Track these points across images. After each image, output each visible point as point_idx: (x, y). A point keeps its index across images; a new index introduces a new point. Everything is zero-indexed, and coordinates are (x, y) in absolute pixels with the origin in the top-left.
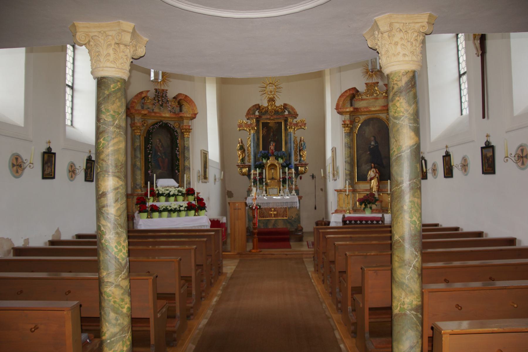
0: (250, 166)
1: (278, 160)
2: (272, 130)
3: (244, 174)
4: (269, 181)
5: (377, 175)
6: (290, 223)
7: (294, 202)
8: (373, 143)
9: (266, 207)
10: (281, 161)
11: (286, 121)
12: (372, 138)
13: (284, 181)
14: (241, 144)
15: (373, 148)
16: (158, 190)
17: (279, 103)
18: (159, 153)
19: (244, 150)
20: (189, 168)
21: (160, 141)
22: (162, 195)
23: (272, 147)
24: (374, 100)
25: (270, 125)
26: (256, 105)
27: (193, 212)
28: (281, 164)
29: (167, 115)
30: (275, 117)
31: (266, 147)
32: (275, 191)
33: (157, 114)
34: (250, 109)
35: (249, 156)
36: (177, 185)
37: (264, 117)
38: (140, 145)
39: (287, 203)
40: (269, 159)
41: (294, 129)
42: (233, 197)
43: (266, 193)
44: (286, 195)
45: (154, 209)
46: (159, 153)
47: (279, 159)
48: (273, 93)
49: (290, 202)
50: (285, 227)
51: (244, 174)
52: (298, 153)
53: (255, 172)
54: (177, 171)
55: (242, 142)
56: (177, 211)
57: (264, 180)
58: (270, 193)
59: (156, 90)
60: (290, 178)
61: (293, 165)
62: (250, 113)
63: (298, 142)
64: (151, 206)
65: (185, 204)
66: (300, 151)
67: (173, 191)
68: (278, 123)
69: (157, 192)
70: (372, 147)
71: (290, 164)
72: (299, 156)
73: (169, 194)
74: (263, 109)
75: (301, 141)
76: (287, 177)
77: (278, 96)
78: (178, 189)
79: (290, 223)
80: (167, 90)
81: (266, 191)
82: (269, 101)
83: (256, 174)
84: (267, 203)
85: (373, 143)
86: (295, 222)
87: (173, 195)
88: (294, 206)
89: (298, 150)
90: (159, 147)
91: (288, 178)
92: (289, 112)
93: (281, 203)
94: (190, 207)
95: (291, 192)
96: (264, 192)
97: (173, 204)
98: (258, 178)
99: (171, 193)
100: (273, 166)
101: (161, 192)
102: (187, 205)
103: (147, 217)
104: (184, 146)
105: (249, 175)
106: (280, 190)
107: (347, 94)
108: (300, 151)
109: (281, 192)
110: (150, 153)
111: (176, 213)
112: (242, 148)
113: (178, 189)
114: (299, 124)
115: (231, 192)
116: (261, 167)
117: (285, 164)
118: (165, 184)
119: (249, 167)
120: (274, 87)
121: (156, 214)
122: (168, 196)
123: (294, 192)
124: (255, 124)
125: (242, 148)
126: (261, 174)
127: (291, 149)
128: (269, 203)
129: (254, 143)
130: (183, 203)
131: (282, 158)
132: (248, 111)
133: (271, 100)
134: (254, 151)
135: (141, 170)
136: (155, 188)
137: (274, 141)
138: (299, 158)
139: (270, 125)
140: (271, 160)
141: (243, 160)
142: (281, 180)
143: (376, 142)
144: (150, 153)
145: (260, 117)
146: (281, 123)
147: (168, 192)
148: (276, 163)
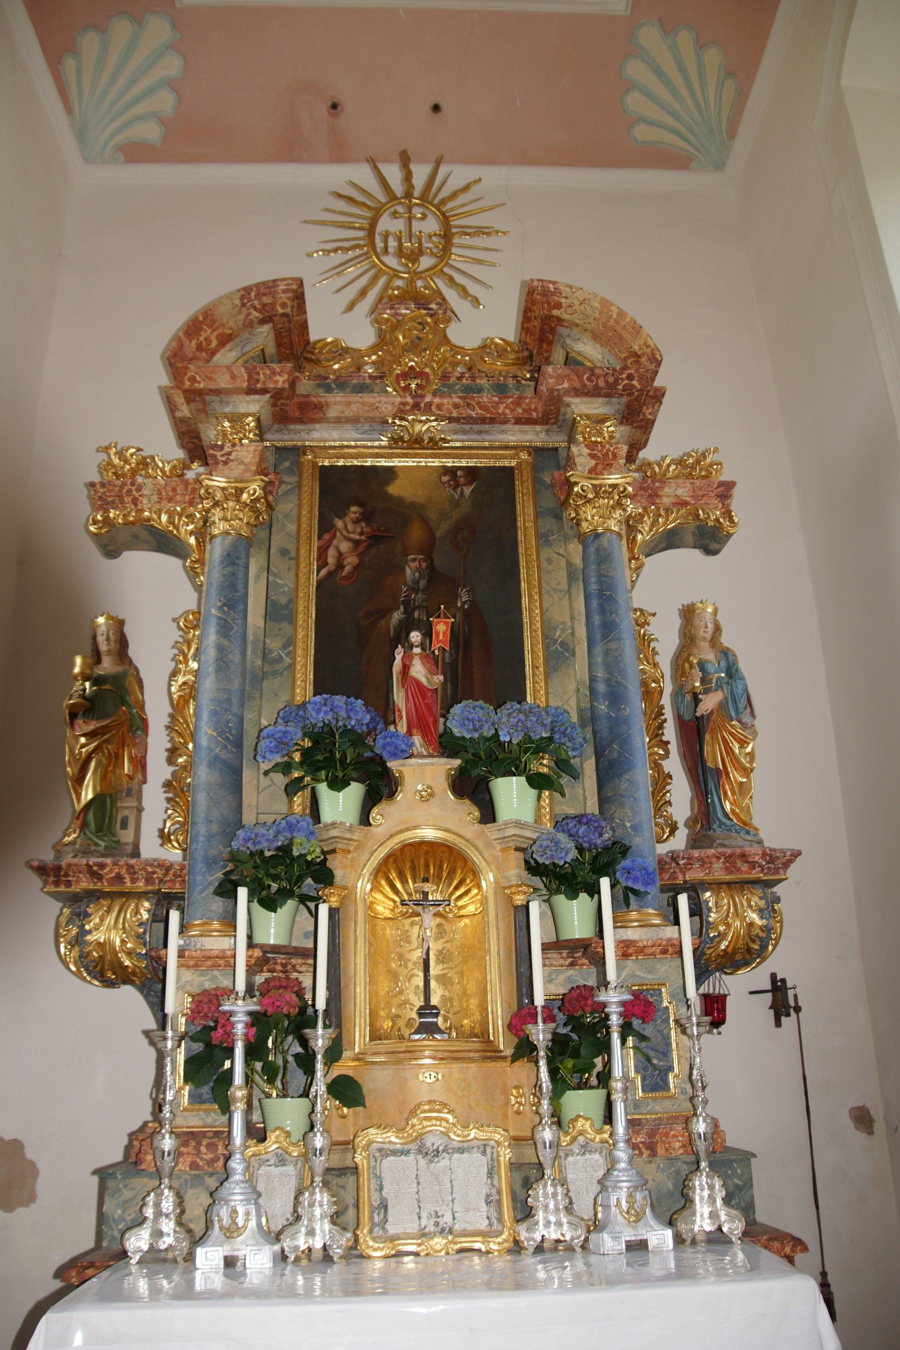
1: (488, 814)
2: (416, 533)
3: (104, 970)
25: (394, 489)
26: (269, 287)
31: (351, 653)
32: (466, 1186)
40: (380, 786)
53: (216, 943)
55: (122, 643)
57: (320, 1038)
63: (665, 661)
68: (472, 473)
76: (613, 999)
83: (227, 961)
91: (629, 1010)
100: (426, 865)
105: (152, 983)
108: (694, 732)
131: (538, 782)
139: (394, 489)
142: (540, 1033)
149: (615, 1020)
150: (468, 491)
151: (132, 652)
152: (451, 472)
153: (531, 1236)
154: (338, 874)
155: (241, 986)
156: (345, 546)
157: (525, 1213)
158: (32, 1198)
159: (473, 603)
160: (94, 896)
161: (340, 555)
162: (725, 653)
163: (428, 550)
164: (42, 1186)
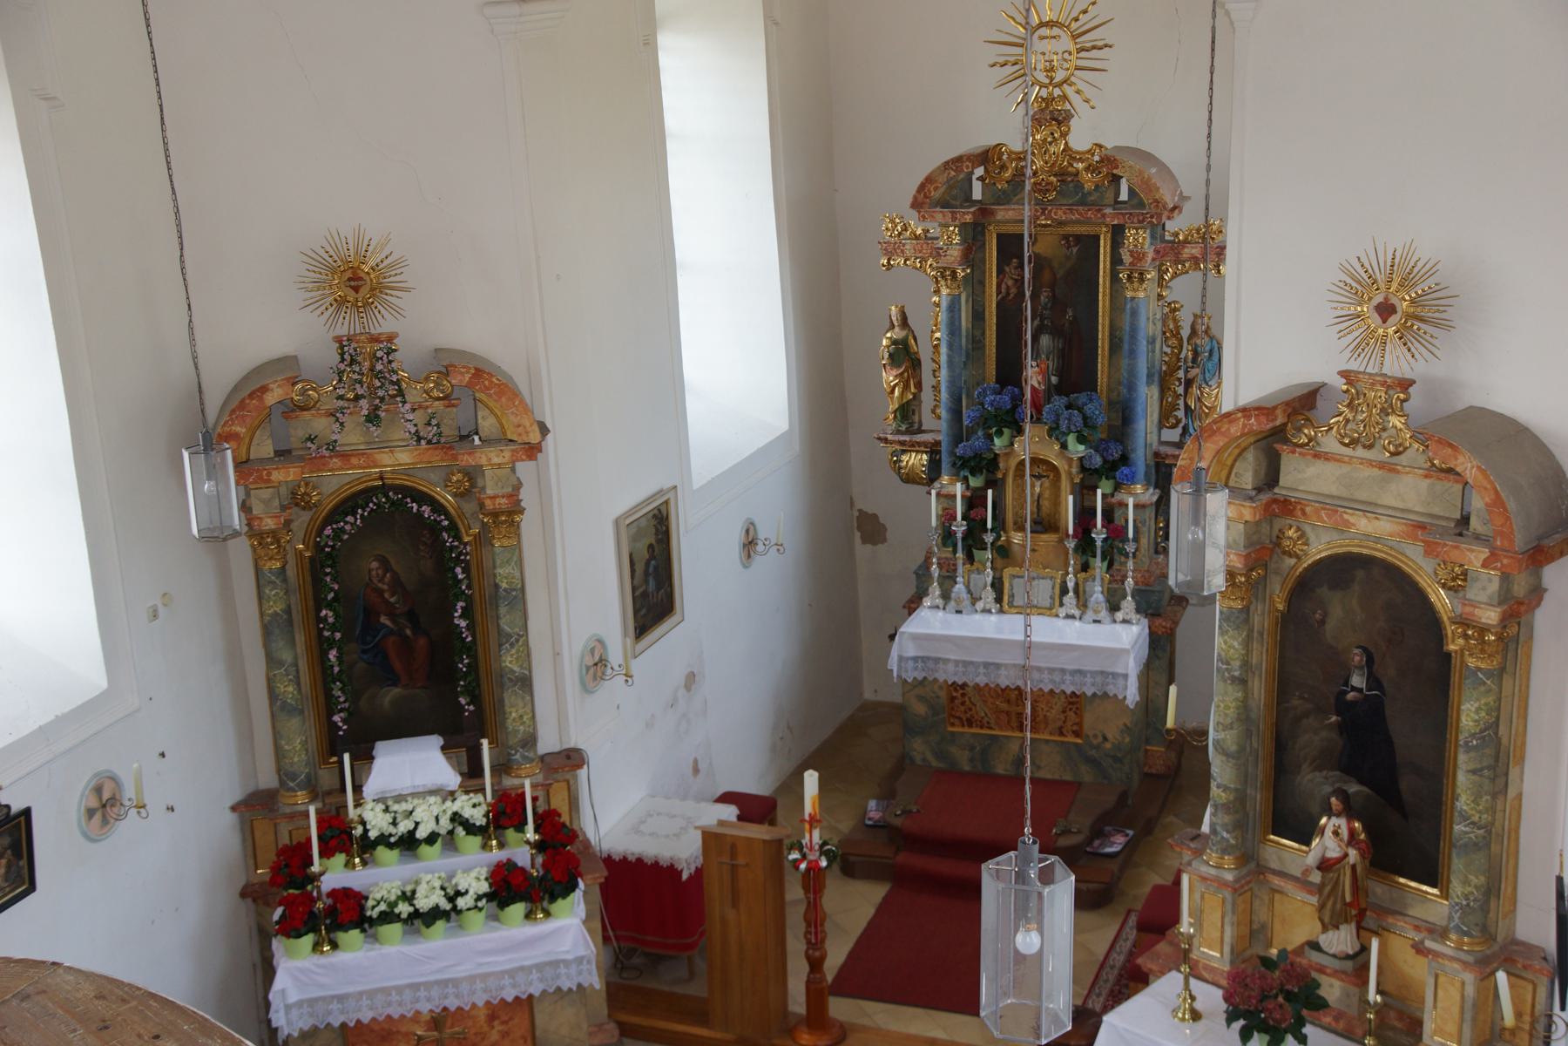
0: (938, 443)
3: (909, 478)
4: (1017, 538)
5: (1353, 854)
6: (1093, 762)
7: (1114, 675)
8: (1357, 680)
9: (981, 680)
10: (1077, 449)
11: (1118, 233)
12: (1357, 657)
13: (1085, 543)
14: (897, 333)
15: (1354, 703)
16: (363, 823)
17: (1080, 137)
18: (384, 620)
19: (916, 364)
20: (526, 683)
21: (384, 563)
22: (383, 840)
23: (1033, 376)
24: (1376, 472)
27: (518, 909)
28: (1081, 459)
29: (404, 457)
30: (1061, 215)
32: (1043, 590)
33: (354, 461)
34: (929, 180)
35: (936, 388)
36: (452, 779)
37: (1003, 213)
38: (288, 611)
39: (1080, 672)
41: (1161, 273)
42: (884, 540)
43: (999, 600)
44: (1090, 615)
45: (349, 913)
46: (384, 620)
47: (1071, 439)
48: (1059, 76)
49: (1094, 674)
50: (1068, 777)
51: (909, 478)
52: (1181, 390)
54: (463, 701)
55: (904, 322)
56: (446, 914)
58: (1018, 601)
59: (339, 340)
60: (1116, 533)
61: (1141, 458)
62: (944, 191)
63: (1185, 333)
64: (333, 893)
65: (475, 882)
66: (1189, 383)
67: (427, 817)
69: (359, 831)
70: (1351, 696)
71: (1125, 459)
72: (1181, 402)
73: (412, 833)
74: (1003, 167)
75: (1194, 332)
77: (1088, 92)
78: (452, 807)
79: (1093, 762)
80: (391, 338)
81: (997, 586)
82: (1037, 122)
84: (986, 665)
85: (1357, 680)
86: (1116, 759)
87: (432, 839)
88: (1111, 690)
89: (1181, 374)
90: (380, 592)
92: (1131, 192)
93: (1051, 670)
94: (507, 888)
95: (1114, 608)
96: (989, 595)
97: (427, 878)
98: (959, 527)
99: (421, 833)
101: (373, 834)
102: (484, 887)
103: (316, 947)
104: (497, 586)
106: (1064, 591)
107: (1235, 430)
109: (1070, 598)
110: (331, 643)
111: (440, 925)
112: (904, 355)
113: (452, 807)
114: (1188, 252)
115: (875, 516)
116: (983, 465)
117: (1098, 461)
118: (411, 774)
119: (933, 450)
120: (1066, 43)
121: (351, 937)
122: (408, 843)
123: (1128, 604)
124: (955, 253)
125: (904, 355)
126: (974, 502)
127: (1132, 387)
128: (998, 666)
129: (950, 346)
130: (471, 870)
131: (1081, 439)
132: (922, 187)
133: (1052, 116)
134: (952, 382)
135: (302, 712)
136: (352, 813)
137: (1056, 332)
138: (1181, 414)
140: (1029, 444)
141: (906, 412)
143: (1373, 681)
144: (331, 643)
145: (984, 211)
146: (1097, 238)
147: (404, 826)
148: (1051, 453)
149: (1099, 543)
150: (1075, 250)
151: (910, 321)
152: (1066, 237)
153: (1062, 612)
154: (1001, 465)
155: (959, 517)
156: (1010, 283)
157: (1061, 605)
158: (884, 540)
159: (1074, 317)
160: (904, 452)
161: (1008, 288)
162: (1212, 338)
163: (1052, 286)
164: (888, 535)
